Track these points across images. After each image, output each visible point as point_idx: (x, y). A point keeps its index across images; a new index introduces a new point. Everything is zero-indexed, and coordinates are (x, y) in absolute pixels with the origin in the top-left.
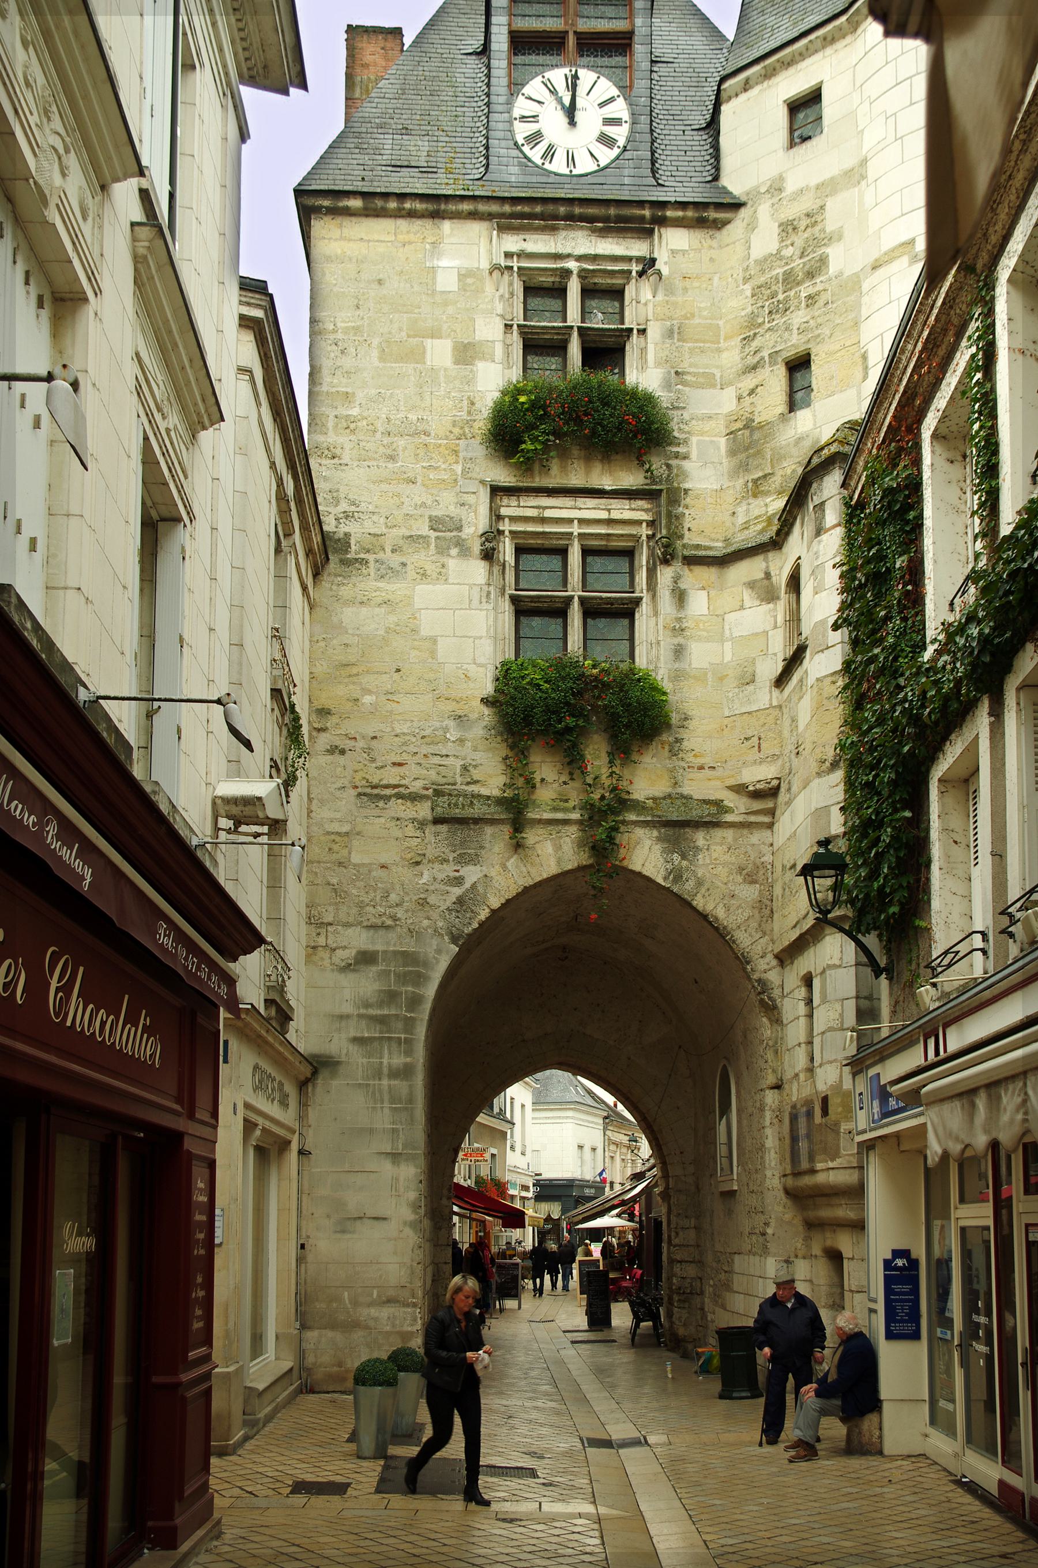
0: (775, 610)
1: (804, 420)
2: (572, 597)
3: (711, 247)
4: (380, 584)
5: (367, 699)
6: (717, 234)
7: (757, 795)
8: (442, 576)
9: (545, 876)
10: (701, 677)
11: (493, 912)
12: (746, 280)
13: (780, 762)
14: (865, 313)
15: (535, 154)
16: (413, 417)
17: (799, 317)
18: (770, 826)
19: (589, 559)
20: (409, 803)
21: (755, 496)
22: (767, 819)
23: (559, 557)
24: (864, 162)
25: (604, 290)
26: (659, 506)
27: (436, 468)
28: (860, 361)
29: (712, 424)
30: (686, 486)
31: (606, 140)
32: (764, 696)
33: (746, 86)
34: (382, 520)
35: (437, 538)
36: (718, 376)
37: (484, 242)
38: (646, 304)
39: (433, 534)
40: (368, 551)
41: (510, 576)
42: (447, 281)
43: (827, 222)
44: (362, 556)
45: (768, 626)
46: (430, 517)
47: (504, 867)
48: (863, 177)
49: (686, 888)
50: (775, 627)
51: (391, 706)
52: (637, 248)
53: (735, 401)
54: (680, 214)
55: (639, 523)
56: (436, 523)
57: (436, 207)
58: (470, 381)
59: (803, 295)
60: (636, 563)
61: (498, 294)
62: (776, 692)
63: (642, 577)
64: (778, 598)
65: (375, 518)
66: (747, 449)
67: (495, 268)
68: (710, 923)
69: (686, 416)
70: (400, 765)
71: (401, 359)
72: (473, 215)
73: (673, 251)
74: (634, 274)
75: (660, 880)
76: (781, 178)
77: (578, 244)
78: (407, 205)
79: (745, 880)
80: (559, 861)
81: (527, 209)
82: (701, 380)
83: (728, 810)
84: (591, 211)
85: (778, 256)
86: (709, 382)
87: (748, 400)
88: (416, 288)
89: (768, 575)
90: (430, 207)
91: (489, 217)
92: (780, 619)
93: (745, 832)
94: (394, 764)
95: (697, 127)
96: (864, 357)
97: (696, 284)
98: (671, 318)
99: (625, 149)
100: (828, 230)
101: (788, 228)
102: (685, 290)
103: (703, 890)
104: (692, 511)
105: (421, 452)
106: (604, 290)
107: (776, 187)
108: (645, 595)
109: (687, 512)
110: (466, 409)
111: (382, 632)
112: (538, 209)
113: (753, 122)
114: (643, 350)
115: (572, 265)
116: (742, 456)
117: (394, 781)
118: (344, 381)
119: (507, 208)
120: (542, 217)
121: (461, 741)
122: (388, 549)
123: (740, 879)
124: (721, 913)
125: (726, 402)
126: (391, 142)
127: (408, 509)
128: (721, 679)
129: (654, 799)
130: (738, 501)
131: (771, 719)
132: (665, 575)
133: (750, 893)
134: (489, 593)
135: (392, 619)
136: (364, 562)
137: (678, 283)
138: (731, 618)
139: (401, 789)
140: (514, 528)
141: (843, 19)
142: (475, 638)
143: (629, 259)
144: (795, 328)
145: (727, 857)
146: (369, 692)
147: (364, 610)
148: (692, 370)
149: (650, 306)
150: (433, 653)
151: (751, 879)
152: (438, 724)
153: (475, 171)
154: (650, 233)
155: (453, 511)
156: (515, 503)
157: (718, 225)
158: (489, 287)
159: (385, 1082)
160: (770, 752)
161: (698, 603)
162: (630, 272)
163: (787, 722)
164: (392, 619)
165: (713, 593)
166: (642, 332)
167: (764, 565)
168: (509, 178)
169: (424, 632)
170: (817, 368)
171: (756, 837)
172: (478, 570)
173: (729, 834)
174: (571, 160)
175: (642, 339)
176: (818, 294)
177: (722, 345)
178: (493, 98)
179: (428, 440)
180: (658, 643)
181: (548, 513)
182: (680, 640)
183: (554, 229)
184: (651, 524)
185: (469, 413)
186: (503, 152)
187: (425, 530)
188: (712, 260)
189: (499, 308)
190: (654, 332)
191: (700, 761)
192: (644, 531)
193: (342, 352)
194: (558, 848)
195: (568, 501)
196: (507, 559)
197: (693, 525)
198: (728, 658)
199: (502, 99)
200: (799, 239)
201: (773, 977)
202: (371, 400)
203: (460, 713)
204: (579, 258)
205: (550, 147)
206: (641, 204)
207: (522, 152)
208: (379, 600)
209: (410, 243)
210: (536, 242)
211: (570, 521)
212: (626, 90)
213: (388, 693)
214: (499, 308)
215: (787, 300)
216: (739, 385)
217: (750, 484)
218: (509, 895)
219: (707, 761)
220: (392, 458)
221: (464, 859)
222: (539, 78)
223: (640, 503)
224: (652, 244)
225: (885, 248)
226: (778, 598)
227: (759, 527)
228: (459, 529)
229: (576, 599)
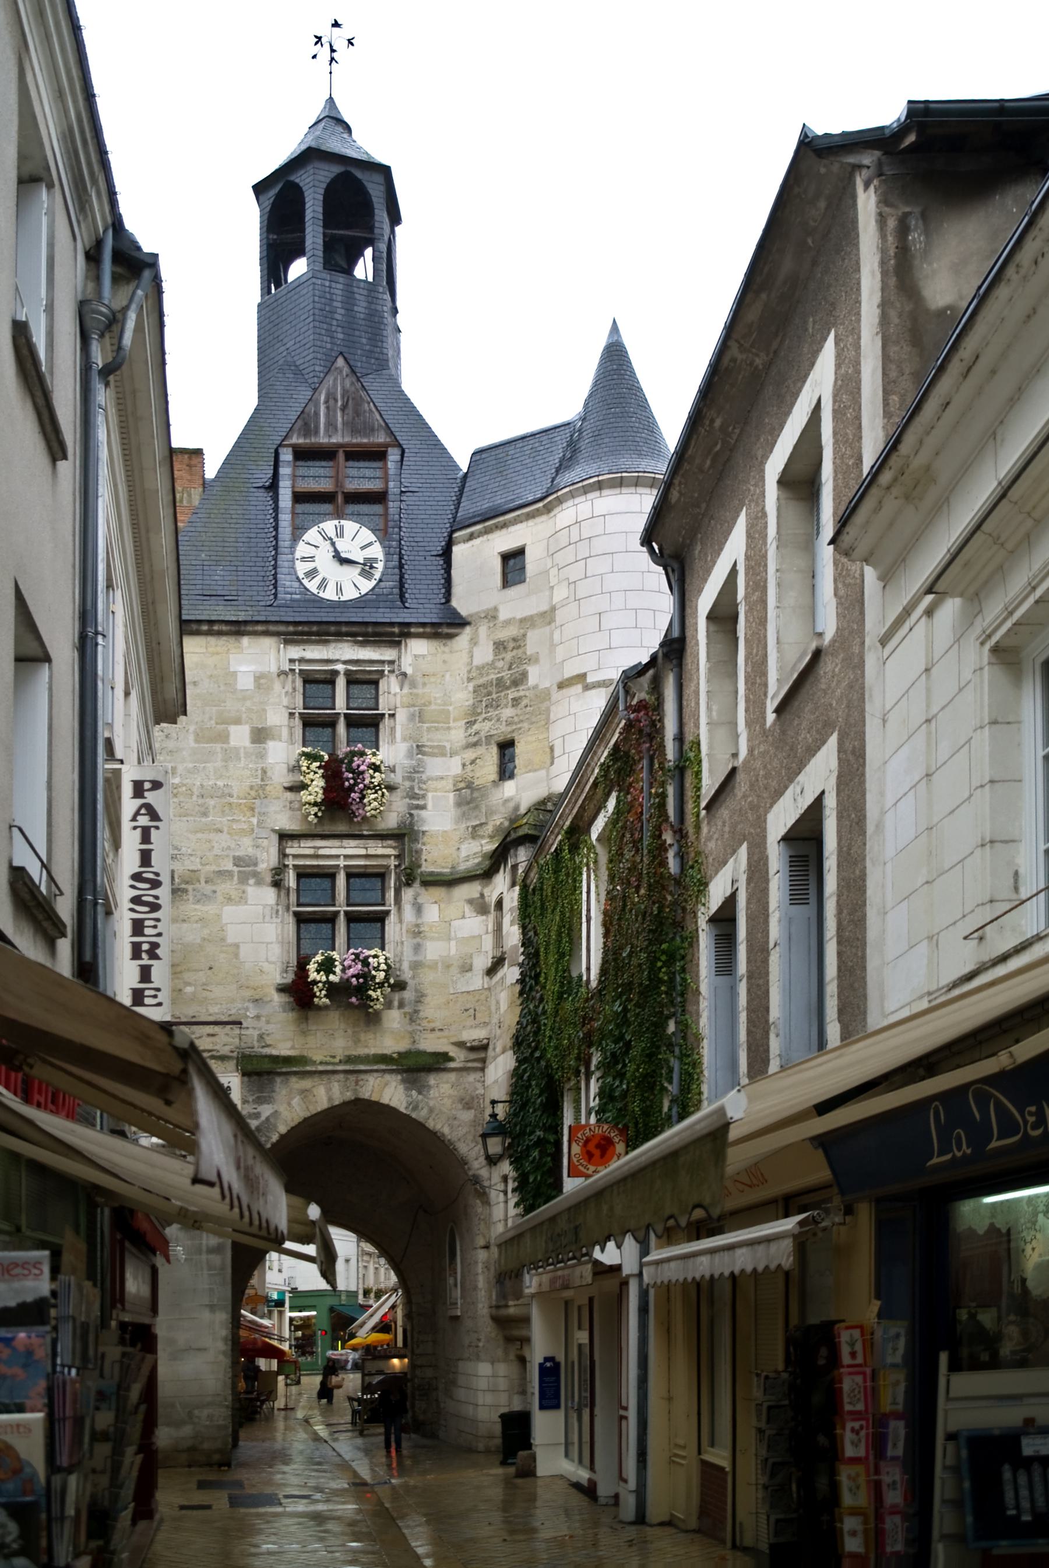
0: (487, 920)
1: (509, 788)
2: (338, 912)
3: (444, 652)
4: (197, 907)
5: (189, 989)
6: (449, 642)
7: (473, 1049)
8: (243, 899)
9: (319, 1110)
10: (433, 966)
11: (283, 1137)
12: (469, 680)
13: (489, 1027)
14: (552, 717)
15: (312, 586)
16: (220, 783)
17: (508, 712)
18: (483, 1069)
19: (352, 880)
20: (220, 1063)
21: (473, 838)
22: (479, 1065)
23: (329, 880)
24: (553, 609)
25: (364, 681)
26: (404, 844)
27: (238, 821)
28: (548, 750)
29: (444, 782)
30: (424, 829)
32: (477, 981)
33: (471, 537)
34: (198, 860)
35: (239, 872)
36: (448, 747)
37: (273, 653)
38: (395, 695)
39: (236, 869)
40: (187, 883)
41: (293, 897)
42: (246, 683)
43: (528, 647)
44: (183, 886)
45: (482, 931)
46: (234, 858)
47: (289, 1104)
48: (552, 620)
49: (420, 1115)
50: (487, 933)
51: (206, 994)
52: (387, 654)
53: (460, 767)
54: (421, 630)
55: (389, 856)
56: (238, 861)
57: (238, 629)
58: (262, 756)
59: (510, 697)
60: (387, 884)
61: (284, 691)
62: (486, 979)
63: (391, 895)
64: (489, 912)
65: (192, 858)
66: (468, 803)
67: (282, 673)
68: (439, 1138)
69: (424, 777)
70: (213, 1035)
71: (211, 740)
72: (266, 633)
73: (415, 656)
74: (386, 672)
75: (402, 1110)
76: (496, 609)
77: (344, 653)
78: (216, 628)
79: (464, 1108)
80: (330, 1099)
81: (306, 629)
82: (436, 751)
83: (451, 1059)
84: (354, 629)
85: (492, 665)
86: (441, 752)
87: (469, 768)
88: (222, 688)
89: (482, 895)
90: (233, 628)
91: (277, 634)
92: (490, 928)
93: (465, 1074)
94: (209, 1035)
95: (435, 553)
96: (552, 749)
97: (432, 680)
98: (413, 706)
99: (380, 580)
100: (528, 653)
101: (500, 646)
102: (424, 684)
103: (433, 1115)
104: (428, 847)
105: (226, 809)
106: (364, 681)
107: (491, 615)
108: (393, 909)
109: (424, 848)
110: (260, 777)
111: (198, 941)
112: (315, 628)
113: (476, 557)
114: (393, 729)
115: (340, 667)
116: (465, 808)
117: (210, 1047)
118: (169, 758)
119: (291, 629)
120: (318, 634)
121: (258, 1017)
122: (203, 881)
123: (460, 1106)
124: (446, 1130)
125: (453, 767)
126: (200, 572)
127: (217, 851)
128: (448, 967)
129: (399, 1053)
130: (461, 840)
131: (483, 997)
132: (408, 894)
133: (467, 1116)
134: (277, 911)
135: (206, 931)
136: (185, 891)
137: (420, 680)
138: (455, 924)
139: (214, 1053)
140: (296, 863)
141: (540, 505)
142: (268, 943)
143: (383, 662)
144: (505, 719)
145: (451, 1092)
146: (189, 984)
147: (185, 925)
148: (429, 744)
149: (398, 696)
150: (236, 955)
151: (468, 1106)
152: (240, 1006)
153: (267, 598)
154: (399, 643)
155: (251, 851)
156: (297, 845)
157: (451, 636)
158: (277, 686)
159: (204, 1257)
160: (483, 1020)
161: (432, 913)
162: (383, 671)
163: (494, 1002)
164: (206, 931)
165: (443, 906)
166: (392, 716)
167: (479, 888)
169: (230, 940)
170: (520, 749)
171: (472, 1077)
172: (270, 895)
173: (452, 1076)
174: (339, 590)
175: (392, 721)
176: (520, 698)
177: (452, 724)
178: (281, 543)
179: (232, 800)
180: (402, 943)
181: (321, 852)
182: (418, 940)
183: (327, 642)
184: (396, 857)
185: (262, 780)
186: (288, 583)
187: (229, 866)
188: (444, 662)
189: (285, 701)
190: (401, 716)
191: (432, 1025)
192: (393, 862)
193: (167, 737)
194: (329, 1090)
195: (336, 843)
196: (291, 885)
197: (429, 857)
198: (453, 952)
199: (287, 544)
200: (509, 656)
201: (484, 1173)
202: (189, 772)
203: (257, 997)
204: (345, 662)
205: (324, 579)
206: (392, 624)
207: (302, 584)
208: (197, 918)
209: (217, 654)
210: (312, 651)
211: (338, 856)
213: (204, 984)
214: (285, 701)
215: (498, 699)
216: (464, 756)
217: (470, 829)
218: (293, 1124)
219: (438, 1025)
220: (205, 814)
221: (260, 1101)
222: (316, 528)
223: (390, 842)
224: (400, 651)
225: (566, 676)
226: (489, 912)
227: (477, 861)
228: (256, 865)
229: (342, 913)
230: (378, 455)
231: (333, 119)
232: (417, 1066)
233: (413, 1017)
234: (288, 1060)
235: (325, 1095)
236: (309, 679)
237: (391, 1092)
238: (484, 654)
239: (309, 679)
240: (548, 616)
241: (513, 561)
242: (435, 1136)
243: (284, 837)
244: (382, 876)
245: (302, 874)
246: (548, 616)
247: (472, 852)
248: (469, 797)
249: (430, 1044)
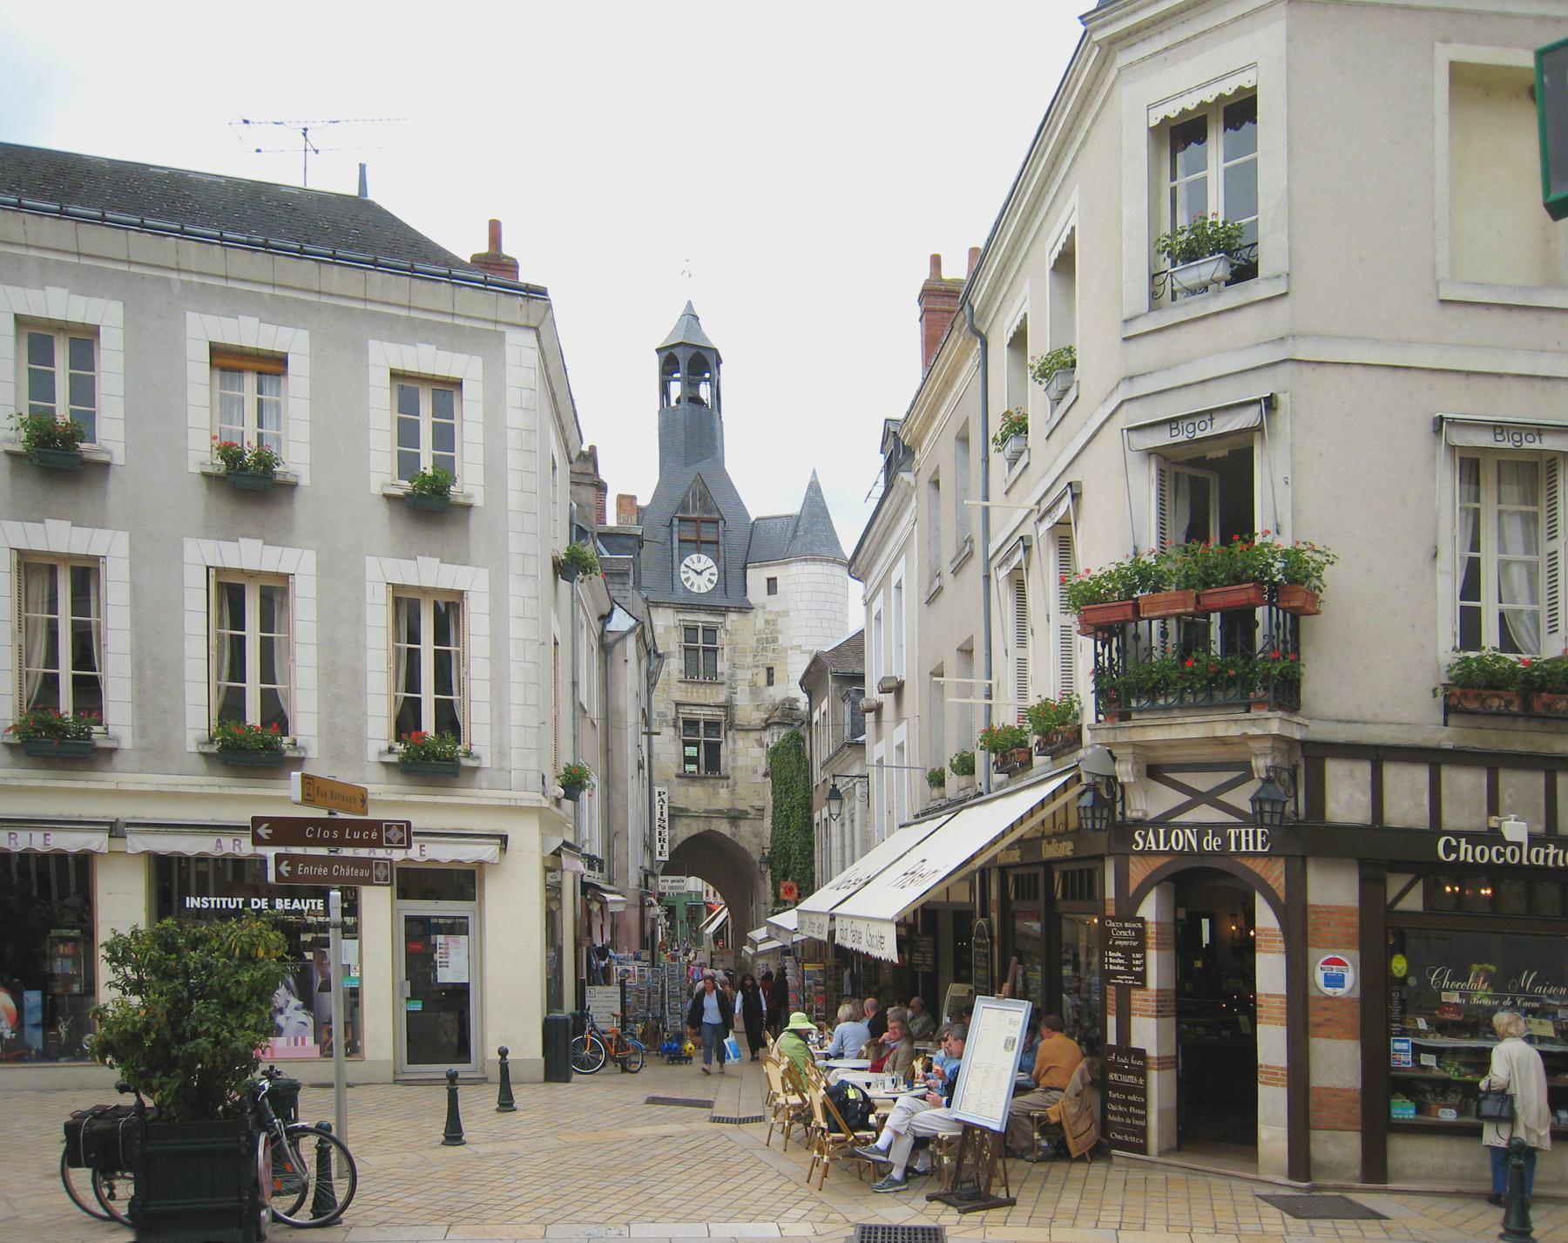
15: (688, 585)
31: (710, 581)
49: (737, 839)
52: (720, 619)
77: (702, 618)
101: (767, 622)
106: (710, 632)
125: (747, 675)
132: (730, 734)
161: (740, 744)
168: (680, 597)
190: (726, 649)
232: (735, 817)
233: (733, 792)
235: (697, 827)
236: (686, 628)
237: (724, 828)
238: (760, 624)
239: (686, 628)
241: (772, 584)
243: (678, 704)
244: (718, 724)
245: (685, 722)
247: (757, 717)
249: (741, 806)
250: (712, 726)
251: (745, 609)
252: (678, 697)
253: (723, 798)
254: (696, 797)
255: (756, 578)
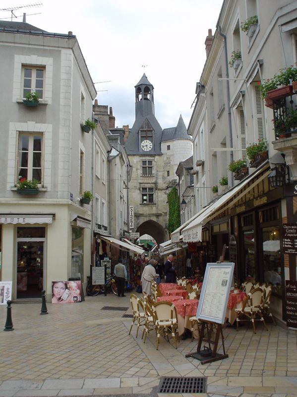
31: (150, 147)
42: (135, 162)
52: (153, 158)
57: (134, 155)
58: (137, 172)
77: (147, 158)
86: (160, 172)
101: (167, 158)
106: (150, 162)
132: (156, 191)
161: (159, 194)
172: (139, 191)
187: (133, 187)
212: (152, 142)
230: (152, 131)
231: (144, 77)
232: (158, 216)
234: (141, 214)
237: (154, 219)
239: (143, 161)
240: (173, 155)
241: (169, 147)
242: (160, 225)
243: (140, 183)
246: (173, 155)
247: (165, 186)
248: (164, 178)
249: (160, 212)
250: (151, 189)
251: (160, 155)
252: (140, 181)
253: (154, 210)
254: (146, 210)
255: (164, 146)
